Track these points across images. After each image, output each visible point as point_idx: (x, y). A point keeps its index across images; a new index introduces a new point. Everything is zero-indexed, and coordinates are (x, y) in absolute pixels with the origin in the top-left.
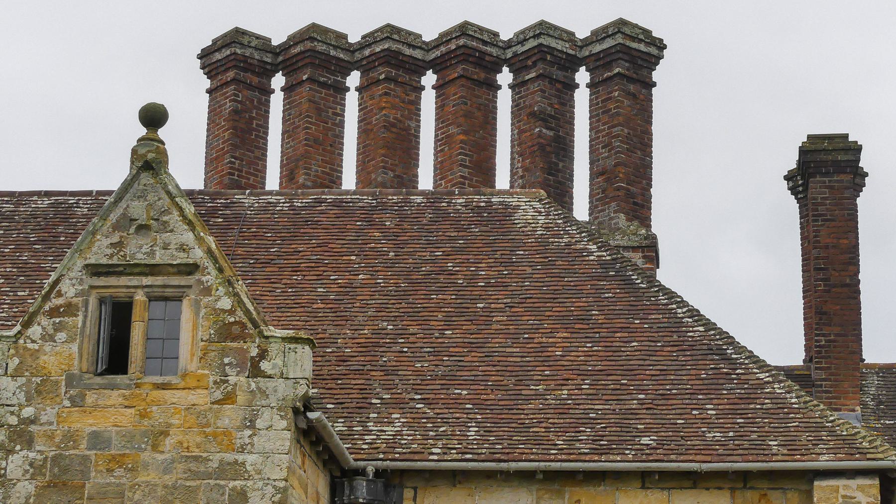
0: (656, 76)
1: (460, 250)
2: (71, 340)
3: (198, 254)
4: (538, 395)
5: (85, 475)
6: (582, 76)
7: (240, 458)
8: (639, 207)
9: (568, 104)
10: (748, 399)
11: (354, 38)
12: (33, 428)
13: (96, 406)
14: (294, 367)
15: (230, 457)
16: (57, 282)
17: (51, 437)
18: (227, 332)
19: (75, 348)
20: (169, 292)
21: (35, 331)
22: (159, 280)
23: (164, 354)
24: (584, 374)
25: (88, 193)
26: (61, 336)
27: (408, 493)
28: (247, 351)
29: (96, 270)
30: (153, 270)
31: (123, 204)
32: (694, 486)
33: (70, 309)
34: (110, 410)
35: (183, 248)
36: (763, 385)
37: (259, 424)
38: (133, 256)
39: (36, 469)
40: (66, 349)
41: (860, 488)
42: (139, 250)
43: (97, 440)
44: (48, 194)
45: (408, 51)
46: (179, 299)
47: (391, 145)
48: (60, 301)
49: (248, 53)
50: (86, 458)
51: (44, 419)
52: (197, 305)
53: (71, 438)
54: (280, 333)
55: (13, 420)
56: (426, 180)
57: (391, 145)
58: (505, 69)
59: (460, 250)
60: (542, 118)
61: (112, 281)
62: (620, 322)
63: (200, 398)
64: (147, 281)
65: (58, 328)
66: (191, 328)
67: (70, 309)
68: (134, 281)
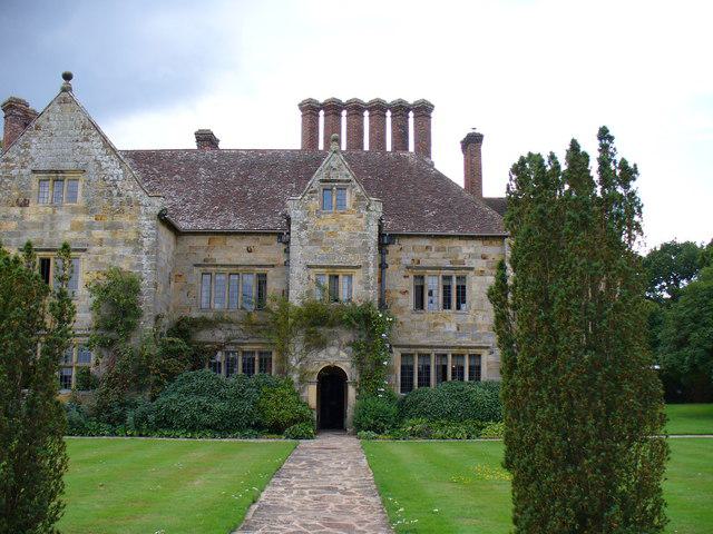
0: (432, 115)
6: (411, 114)
8: (428, 153)
10: (484, 215)
14: (377, 209)
18: (359, 198)
21: (306, 197)
23: (341, 204)
29: (322, 181)
33: (315, 192)
34: (328, 221)
35: (347, 176)
39: (308, 236)
40: (315, 204)
47: (355, 134)
50: (322, 234)
52: (351, 191)
56: (366, 148)
57: (355, 134)
60: (400, 127)
66: (349, 199)
67: (315, 192)
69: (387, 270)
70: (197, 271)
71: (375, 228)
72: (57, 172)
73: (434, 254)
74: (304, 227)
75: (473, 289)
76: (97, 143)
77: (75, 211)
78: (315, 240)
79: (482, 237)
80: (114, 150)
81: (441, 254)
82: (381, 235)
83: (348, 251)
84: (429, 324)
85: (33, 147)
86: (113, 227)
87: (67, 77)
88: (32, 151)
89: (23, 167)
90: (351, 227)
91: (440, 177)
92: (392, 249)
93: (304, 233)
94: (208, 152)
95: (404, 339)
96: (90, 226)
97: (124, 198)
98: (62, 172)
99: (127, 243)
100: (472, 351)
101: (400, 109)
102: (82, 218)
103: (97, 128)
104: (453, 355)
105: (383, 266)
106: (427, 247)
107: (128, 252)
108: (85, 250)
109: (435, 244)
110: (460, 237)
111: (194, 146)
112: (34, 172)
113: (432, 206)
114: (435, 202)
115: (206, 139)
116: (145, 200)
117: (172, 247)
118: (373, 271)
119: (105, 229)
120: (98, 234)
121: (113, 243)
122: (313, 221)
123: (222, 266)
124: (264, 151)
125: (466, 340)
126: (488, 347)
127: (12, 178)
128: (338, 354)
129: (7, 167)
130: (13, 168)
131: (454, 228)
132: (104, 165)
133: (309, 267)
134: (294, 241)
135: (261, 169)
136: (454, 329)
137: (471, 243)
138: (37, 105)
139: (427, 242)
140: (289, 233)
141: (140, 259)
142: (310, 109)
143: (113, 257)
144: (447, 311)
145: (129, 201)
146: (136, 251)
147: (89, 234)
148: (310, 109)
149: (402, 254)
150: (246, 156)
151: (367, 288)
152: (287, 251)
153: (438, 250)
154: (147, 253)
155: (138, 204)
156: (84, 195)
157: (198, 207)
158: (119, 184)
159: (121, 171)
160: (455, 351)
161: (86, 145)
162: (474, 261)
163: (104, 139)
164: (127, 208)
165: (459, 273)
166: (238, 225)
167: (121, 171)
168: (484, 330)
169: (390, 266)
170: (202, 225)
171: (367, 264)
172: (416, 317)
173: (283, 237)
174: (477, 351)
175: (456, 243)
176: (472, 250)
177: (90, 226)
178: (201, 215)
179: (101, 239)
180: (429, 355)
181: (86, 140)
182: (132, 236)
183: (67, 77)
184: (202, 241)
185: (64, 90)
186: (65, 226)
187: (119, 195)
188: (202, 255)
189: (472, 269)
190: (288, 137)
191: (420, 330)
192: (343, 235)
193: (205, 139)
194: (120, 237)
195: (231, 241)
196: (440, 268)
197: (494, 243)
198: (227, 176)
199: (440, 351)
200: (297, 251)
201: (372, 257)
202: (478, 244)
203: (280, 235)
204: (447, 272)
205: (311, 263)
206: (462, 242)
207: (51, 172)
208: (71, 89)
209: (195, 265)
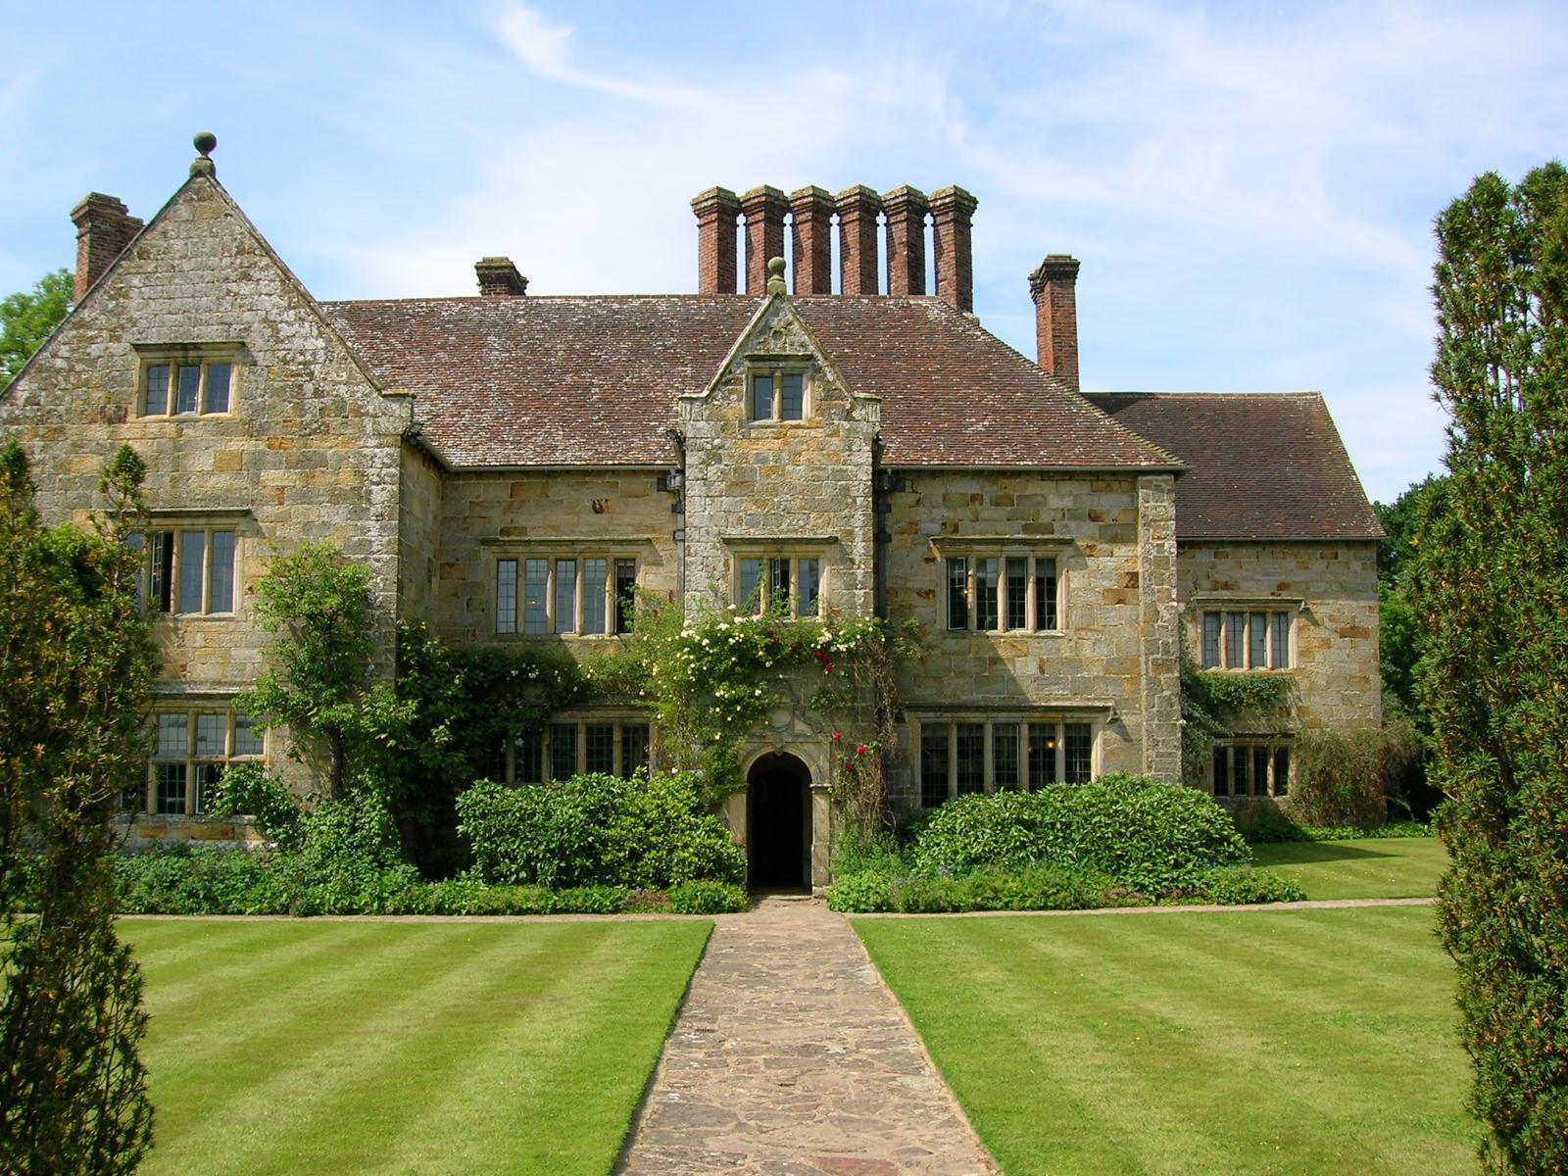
0: (973, 220)
1: (900, 335)
2: (739, 400)
3: (812, 349)
4: (972, 424)
5: (754, 482)
7: (844, 467)
9: (922, 236)
11: (787, 194)
12: (721, 451)
13: (758, 439)
14: (869, 418)
15: (837, 467)
16: (728, 365)
17: (731, 457)
18: (830, 395)
19: (743, 405)
20: (795, 372)
22: (791, 363)
23: (791, 409)
24: (995, 412)
25: (664, 296)
26: (734, 397)
27: (908, 483)
28: (844, 406)
29: (753, 358)
30: (787, 358)
31: (764, 319)
32: (1070, 479)
34: (764, 442)
35: (802, 345)
36: (1098, 420)
37: (855, 448)
38: (773, 350)
40: (736, 406)
41: (1163, 481)
42: (775, 347)
43: (761, 459)
44: (639, 297)
45: (824, 202)
46: (801, 375)
48: (730, 377)
49: (725, 202)
51: (727, 446)
53: (744, 457)
54: (862, 395)
55: (709, 447)
58: (881, 214)
59: (900, 335)
61: (761, 364)
62: (1007, 380)
63: (818, 433)
64: (781, 364)
65: (731, 392)
68: (774, 364)
69: (890, 547)
70: (487, 554)
71: (865, 457)
72: (184, 347)
73: (987, 512)
74: (714, 456)
75: (1072, 586)
76: (268, 282)
77: (224, 430)
78: (740, 484)
79: (1089, 473)
80: (306, 299)
81: (1002, 512)
82: (878, 473)
83: (813, 506)
84: (980, 660)
85: (134, 293)
86: (307, 463)
87: (206, 144)
88: (134, 303)
89: (115, 338)
90: (815, 456)
91: (997, 347)
92: (901, 501)
93: (713, 471)
94: (507, 303)
95: (926, 693)
96: (258, 463)
97: (328, 400)
98: (196, 346)
99: (336, 496)
100: (1072, 718)
101: (914, 206)
102: (237, 444)
103: (268, 251)
104: (1032, 726)
105: (880, 538)
106: (974, 498)
107: (338, 515)
108: (247, 513)
109: (989, 490)
110: (1044, 475)
111: (472, 288)
112: (137, 347)
113: (982, 412)
114: (989, 399)
115: (500, 278)
116: (375, 403)
117: (434, 504)
118: (861, 548)
119: (290, 466)
120: (273, 477)
121: (306, 497)
122: (734, 447)
123: (540, 542)
124: (622, 299)
125: (1059, 697)
126: (1106, 709)
127: (92, 362)
128: (790, 726)
129: (81, 339)
130: (92, 340)
131: (1030, 450)
132: (285, 330)
133: (728, 542)
134: (694, 490)
135: (619, 338)
136: (1032, 668)
137: (1066, 486)
138: (142, 208)
139: (972, 487)
140: (682, 472)
141: (364, 531)
142: (721, 212)
143: (307, 527)
144: (1017, 632)
145: (340, 406)
146: (359, 513)
147: (256, 481)
148: (721, 212)
149: (921, 513)
150: (586, 311)
151: (851, 586)
152: (678, 509)
153: (996, 503)
154: (380, 517)
155: (359, 412)
156: (244, 396)
157: (487, 418)
158: (317, 368)
159: (321, 343)
160: (1037, 717)
161: (246, 288)
162: (1073, 525)
163: (286, 275)
164: (334, 421)
165: (1042, 552)
166: (572, 454)
167: (321, 343)
168: (1096, 671)
169: (895, 539)
170: (496, 456)
171: (850, 533)
172: (951, 644)
173: (666, 482)
174: (1085, 718)
175: (1034, 487)
176: (1068, 503)
177: (258, 463)
178: (494, 436)
179: (282, 489)
180: (980, 727)
181: (246, 277)
182: (346, 480)
183: (206, 144)
184: (499, 491)
185: (197, 173)
186: (203, 461)
187: (318, 393)
188: (498, 520)
189: (1070, 542)
190: (669, 265)
191: (960, 674)
192: (798, 472)
193: (499, 279)
194: (323, 480)
195: (558, 489)
196: (1001, 542)
197: (1115, 485)
198: (547, 353)
199: (1004, 717)
200: (698, 508)
201: (860, 521)
202: (1082, 488)
203: (662, 478)
204: (1015, 551)
205: (733, 532)
206: (1048, 484)
207: (172, 347)
208: (212, 171)
209: (485, 542)
